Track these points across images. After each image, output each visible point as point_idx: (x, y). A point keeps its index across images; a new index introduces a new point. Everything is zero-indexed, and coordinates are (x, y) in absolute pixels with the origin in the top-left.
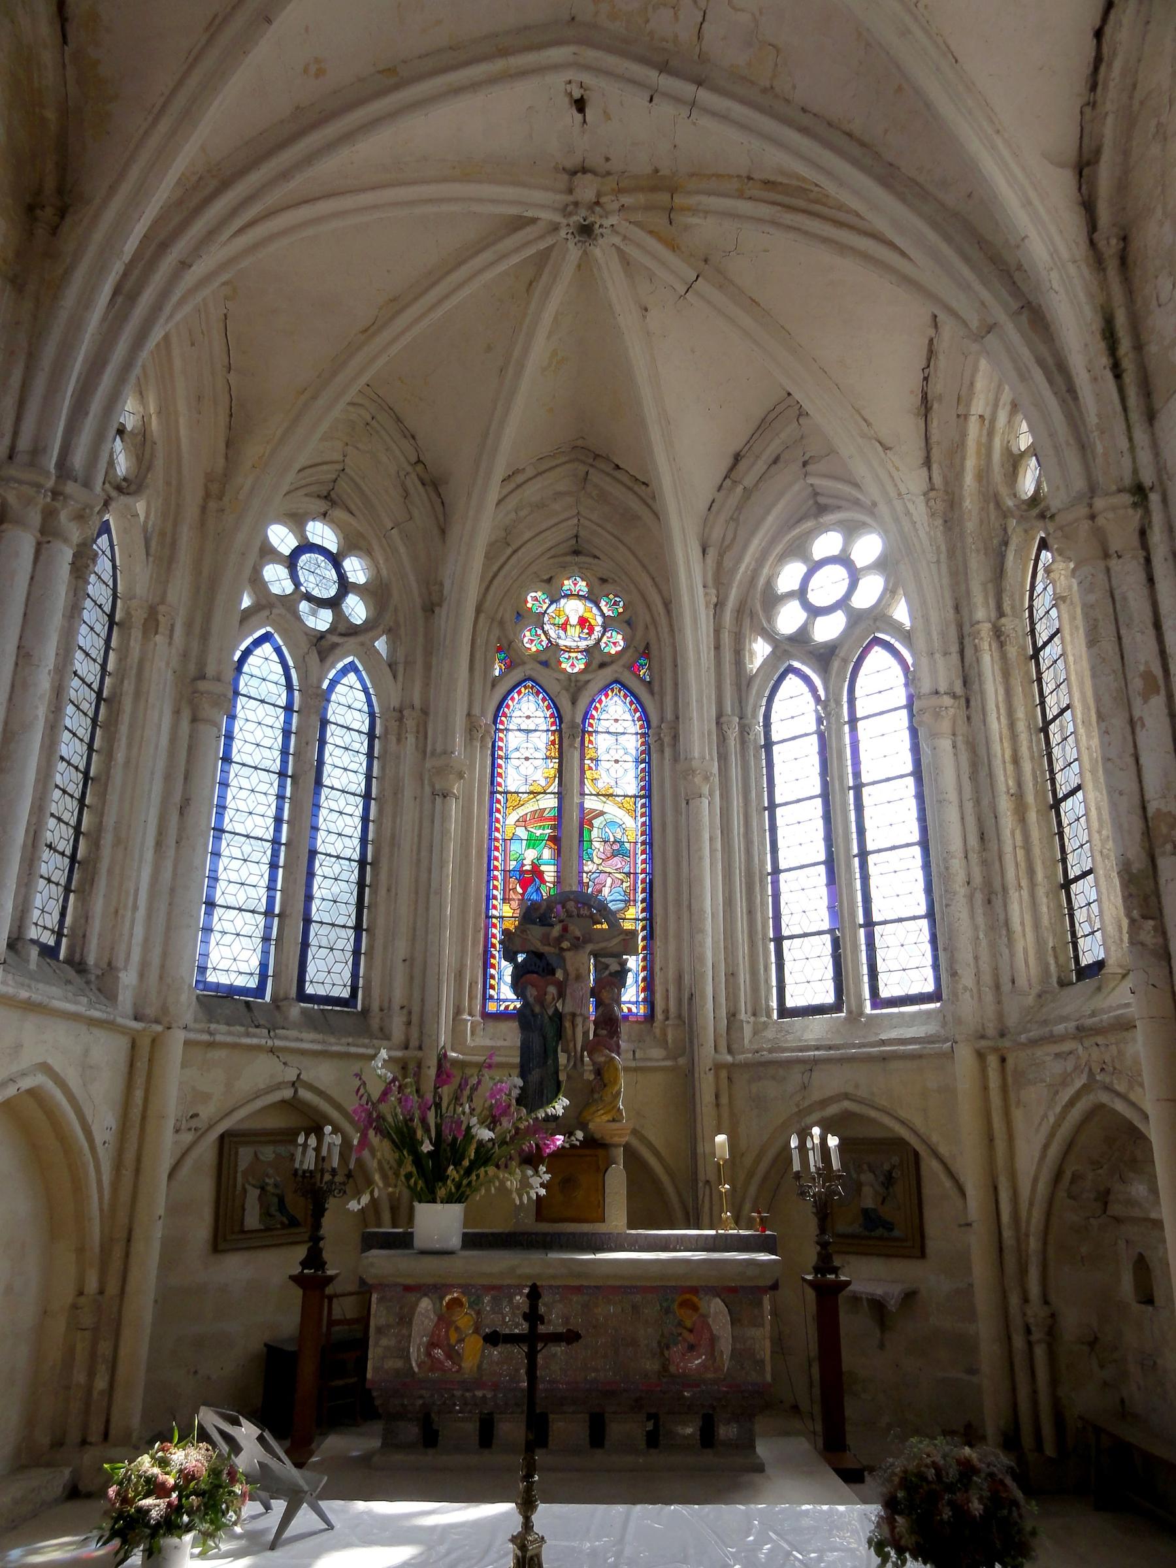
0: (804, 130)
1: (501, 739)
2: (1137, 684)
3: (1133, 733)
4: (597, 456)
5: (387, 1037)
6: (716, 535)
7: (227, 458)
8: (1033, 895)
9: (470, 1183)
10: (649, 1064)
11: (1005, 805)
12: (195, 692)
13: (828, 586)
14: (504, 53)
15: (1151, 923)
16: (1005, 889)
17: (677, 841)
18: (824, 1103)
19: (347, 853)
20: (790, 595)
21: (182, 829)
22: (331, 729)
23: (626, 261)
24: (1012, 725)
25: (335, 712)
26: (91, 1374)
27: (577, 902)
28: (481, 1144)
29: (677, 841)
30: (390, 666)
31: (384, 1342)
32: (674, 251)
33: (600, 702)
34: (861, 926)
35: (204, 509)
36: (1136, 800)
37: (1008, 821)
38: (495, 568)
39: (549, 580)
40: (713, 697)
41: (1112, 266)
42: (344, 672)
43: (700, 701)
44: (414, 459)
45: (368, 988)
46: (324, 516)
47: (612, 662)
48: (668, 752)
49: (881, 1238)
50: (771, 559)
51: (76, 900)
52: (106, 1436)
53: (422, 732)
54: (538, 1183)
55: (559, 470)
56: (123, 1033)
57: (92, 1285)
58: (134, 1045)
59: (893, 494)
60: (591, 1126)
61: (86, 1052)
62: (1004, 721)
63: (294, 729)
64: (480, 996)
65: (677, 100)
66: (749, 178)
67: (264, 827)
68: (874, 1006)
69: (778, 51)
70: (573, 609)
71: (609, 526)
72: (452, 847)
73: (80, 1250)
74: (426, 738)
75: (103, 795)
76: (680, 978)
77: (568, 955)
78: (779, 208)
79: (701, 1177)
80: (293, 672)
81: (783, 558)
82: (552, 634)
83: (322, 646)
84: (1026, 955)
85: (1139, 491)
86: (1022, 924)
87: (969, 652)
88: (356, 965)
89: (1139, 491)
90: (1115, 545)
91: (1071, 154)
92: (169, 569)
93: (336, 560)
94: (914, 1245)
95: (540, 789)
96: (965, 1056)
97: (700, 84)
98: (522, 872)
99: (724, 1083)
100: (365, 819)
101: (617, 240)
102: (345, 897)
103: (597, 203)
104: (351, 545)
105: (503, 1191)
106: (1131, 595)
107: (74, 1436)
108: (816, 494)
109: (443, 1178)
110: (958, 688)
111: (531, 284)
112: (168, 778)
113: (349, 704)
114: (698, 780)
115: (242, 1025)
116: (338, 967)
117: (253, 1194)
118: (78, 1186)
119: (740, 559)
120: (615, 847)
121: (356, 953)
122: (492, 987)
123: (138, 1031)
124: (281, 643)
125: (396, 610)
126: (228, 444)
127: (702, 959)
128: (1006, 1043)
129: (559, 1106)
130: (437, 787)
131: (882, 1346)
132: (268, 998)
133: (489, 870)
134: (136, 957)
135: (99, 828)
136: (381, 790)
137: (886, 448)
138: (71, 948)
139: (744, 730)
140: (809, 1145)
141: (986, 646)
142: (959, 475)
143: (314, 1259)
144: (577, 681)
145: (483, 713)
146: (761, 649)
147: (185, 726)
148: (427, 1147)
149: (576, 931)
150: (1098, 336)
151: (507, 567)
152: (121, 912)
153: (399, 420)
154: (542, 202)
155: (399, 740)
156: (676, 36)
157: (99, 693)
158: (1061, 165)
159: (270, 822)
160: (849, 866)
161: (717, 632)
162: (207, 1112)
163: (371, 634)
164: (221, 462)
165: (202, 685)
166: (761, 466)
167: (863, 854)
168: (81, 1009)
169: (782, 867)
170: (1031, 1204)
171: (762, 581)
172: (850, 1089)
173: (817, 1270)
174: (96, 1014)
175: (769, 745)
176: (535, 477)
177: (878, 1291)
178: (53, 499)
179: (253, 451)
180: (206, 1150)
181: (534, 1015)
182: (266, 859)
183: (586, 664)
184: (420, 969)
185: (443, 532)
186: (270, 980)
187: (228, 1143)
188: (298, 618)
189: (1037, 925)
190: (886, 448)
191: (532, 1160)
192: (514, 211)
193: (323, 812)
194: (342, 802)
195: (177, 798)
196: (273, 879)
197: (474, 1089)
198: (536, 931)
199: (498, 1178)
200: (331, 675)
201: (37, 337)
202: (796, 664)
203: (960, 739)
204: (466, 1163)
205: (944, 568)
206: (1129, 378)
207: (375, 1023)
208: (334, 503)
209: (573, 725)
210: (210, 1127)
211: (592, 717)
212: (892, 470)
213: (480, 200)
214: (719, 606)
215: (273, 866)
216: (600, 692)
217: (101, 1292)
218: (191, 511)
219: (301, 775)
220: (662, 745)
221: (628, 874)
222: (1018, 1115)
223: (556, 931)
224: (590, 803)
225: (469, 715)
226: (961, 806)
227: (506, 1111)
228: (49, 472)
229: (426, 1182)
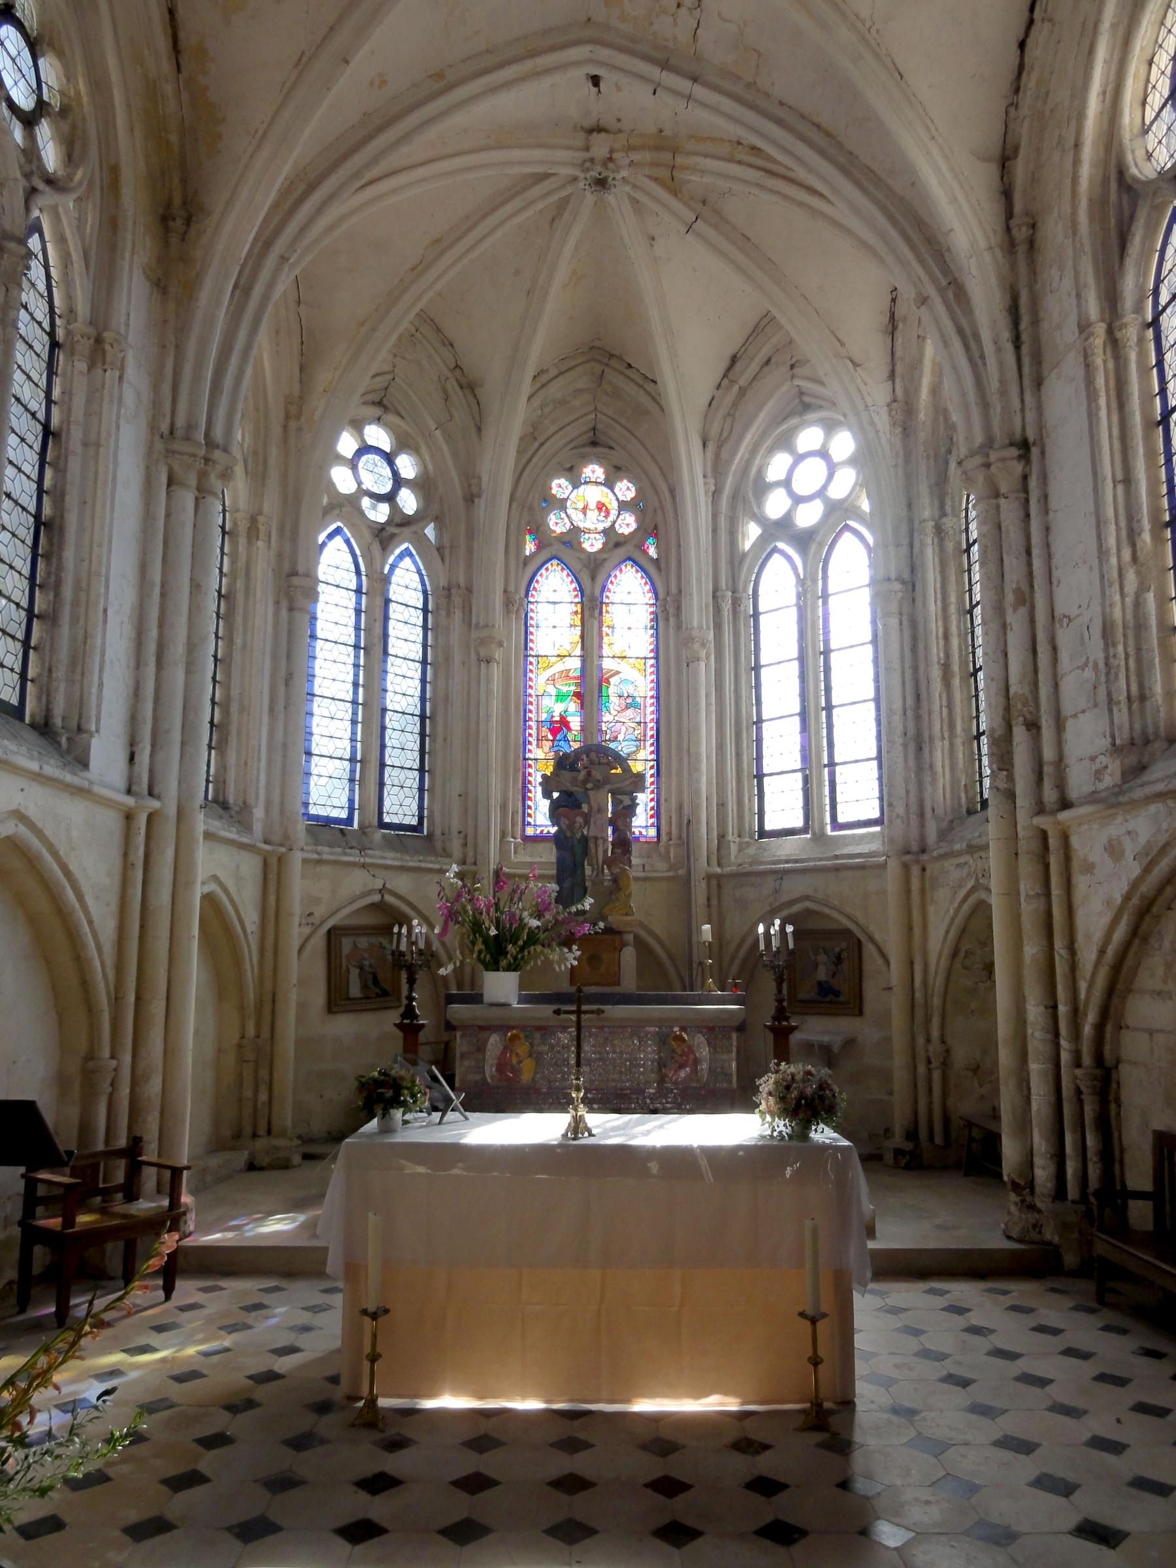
0: (780, 122)
1: (532, 610)
2: (1010, 597)
3: (1005, 634)
4: (611, 356)
6: (714, 431)
7: (301, 382)
8: (952, 745)
9: (523, 957)
10: (655, 875)
11: (936, 673)
12: (290, 586)
13: (809, 477)
14: (533, 54)
15: (1005, 773)
16: (931, 739)
18: (791, 903)
19: (410, 710)
20: (777, 484)
21: (288, 697)
22: (392, 606)
23: (635, 202)
24: (945, 608)
25: (395, 592)
26: (256, 1091)
27: (598, 752)
28: (531, 931)
29: (679, 695)
30: (438, 550)
31: (467, 1063)
32: (676, 195)
33: (615, 576)
34: (825, 766)
35: (285, 427)
36: (1002, 685)
37: (937, 686)
39: (571, 469)
40: (711, 575)
41: (1022, 249)
42: (401, 557)
43: (699, 580)
44: (452, 365)
45: (430, 817)
46: (378, 420)
47: (625, 542)
48: (672, 620)
49: (830, 1002)
50: (762, 451)
51: (216, 755)
52: (269, 1132)
53: (467, 609)
54: (572, 957)
55: (579, 369)
56: (258, 854)
57: (251, 1031)
58: (266, 864)
59: (861, 407)
60: (610, 918)
62: (939, 603)
63: (363, 608)
64: (520, 823)
65: (676, 93)
66: (739, 143)
67: (345, 691)
68: (834, 829)
69: (760, 55)
70: (593, 494)
71: (623, 421)
72: (495, 705)
73: (242, 1008)
74: (471, 612)
75: (228, 675)
76: (680, 807)
77: (591, 793)
78: (762, 173)
79: (695, 959)
80: (360, 560)
81: (771, 451)
82: (574, 517)
83: (383, 537)
84: (941, 791)
85: (1024, 446)
86: (943, 766)
87: (917, 545)
88: (421, 799)
89: (1024, 446)
90: (1004, 489)
91: (996, 150)
92: (263, 485)
93: (389, 459)
94: (857, 1007)
95: (566, 653)
96: (894, 866)
97: (695, 80)
98: (552, 722)
99: (714, 891)
100: (423, 681)
101: (628, 188)
102: (410, 745)
103: (610, 159)
104: (403, 444)
105: (548, 963)
106: (1011, 528)
107: (248, 1130)
108: (801, 393)
109: (504, 953)
110: (906, 576)
111: (553, 220)
112: (275, 656)
113: (406, 583)
114: (696, 646)
115: (339, 847)
116: (408, 801)
118: (238, 963)
119: (733, 454)
120: (629, 701)
121: (421, 789)
122: (530, 815)
123: (268, 852)
124: (349, 535)
125: (441, 500)
126: (302, 369)
127: (697, 793)
128: (925, 857)
130: (482, 654)
132: (356, 826)
133: (525, 721)
134: (262, 798)
135: (228, 698)
136: (435, 656)
137: (856, 365)
138: (216, 791)
139: (736, 602)
140: (772, 932)
141: (929, 541)
142: (917, 390)
143: (409, 1013)
144: (596, 560)
145: (517, 591)
146: (753, 531)
147: (284, 613)
149: (597, 775)
150: (1005, 313)
151: (535, 460)
152: (250, 763)
153: (439, 330)
154: (563, 161)
155: (448, 614)
156: (675, 38)
158: (988, 160)
159: (350, 687)
160: (818, 717)
161: (715, 516)
162: (319, 911)
163: (421, 525)
164: (297, 385)
165: (296, 581)
166: (753, 368)
167: (829, 708)
169: (764, 718)
170: (936, 973)
171: (753, 471)
172: (810, 892)
173: (774, 1018)
175: (756, 615)
176: (557, 376)
177: (826, 1039)
178: (205, 464)
179: (323, 377)
180: (319, 941)
181: (566, 838)
182: (349, 716)
184: (470, 803)
185: (479, 429)
186: (356, 813)
187: (333, 935)
188: (362, 513)
189: (953, 768)
190: (856, 365)
191: (567, 942)
192: (540, 169)
193: (390, 677)
194: (404, 667)
195: (282, 673)
196: (354, 733)
197: (522, 893)
198: (567, 776)
199: (542, 952)
200: (391, 560)
201: (182, 330)
202: (781, 545)
203: (905, 618)
204: (521, 943)
205: (901, 472)
206: (1025, 349)
207: (438, 845)
208: (386, 409)
209: (593, 599)
210: (322, 923)
211: (609, 590)
212: (862, 386)
213: (509, 163)
214: (716, 494)
215: (354, 722)
216: (615, 567)
217: (258, 1036)
218: (276, 431)
219: (372, 645)
220: (668, 614)
221: (639, 723)
222: (931, 909)
223: (582, 775)
225: (505, 591)
226: (903, 673)
227: (547, 908)
228: (200, 444)
229: (492, 956)
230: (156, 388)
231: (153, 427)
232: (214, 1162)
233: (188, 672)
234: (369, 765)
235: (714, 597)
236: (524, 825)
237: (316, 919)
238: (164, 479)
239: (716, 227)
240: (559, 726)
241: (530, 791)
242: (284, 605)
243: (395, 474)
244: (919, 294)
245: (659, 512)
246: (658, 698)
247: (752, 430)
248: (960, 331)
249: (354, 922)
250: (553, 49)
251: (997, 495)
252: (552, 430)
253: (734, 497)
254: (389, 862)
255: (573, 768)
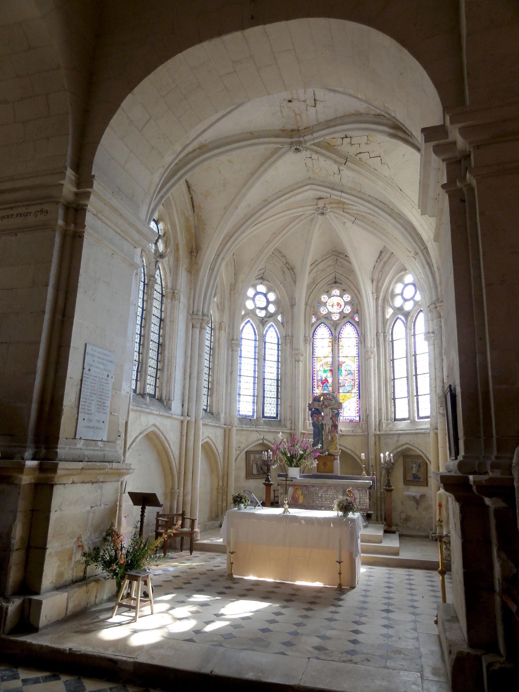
0: (368, 202)
5: (286, 427)
17: (365, 370)
18: (403, 445)
20: (398, 294)
21: (231, 378)
22: (267, 344)
26: (222, 503)
38: (311, 291)
39: (328, 292)
42: (270, 327)
43: (370, 330)
49: (417, 481)
53: (292, 343)
57: (221, 484)
61: (215, 433)
68: (418, 419)
71: (344, 275)
73: (218, 476)
79: (370, 464)
81: (396, 283)
83: (263, 322)
88: (277, 408)
93: (265, 295)
96: (432, 434)
97: (342, 192)
100: (278, 368)
102: (273, 390)
104: (270, 290)
109: (293, 462)
112: (227, 366)
113: (272, 335)
114: (369, 353)
117: (255, 466)
118: (216, 463)
119: (383, 284)
121: (277, 405)
124: (252, 322)
127: (371, 405)
129: (320, 446)
131: (417, 509)
134: (224, 410)
135: (213, 380)
136: (281, 360)
138: (210, 409)
139: (385, 337)
143: (267, 480)
146: (390, 312)
147: (230, 352)
148: (289, 455)
149: (326, 403)
151: (314, 290)
155: (286, 345)
157: (210, 348)
161: (377, 307)
162: (242, 446)
164: (234, 280)
165: (233, 342)
168: (214, 424)
174: (217, 425)
175: (392, 341)
177: (414, 494)
180: (243, 455)
183: (340, 317)
185: (295, 282)
188: (256, 315)
193: (266, 368)
195: (230, 371)
196: (254, 387)
198: (316, 403)
201: (195, 284)
202: (400, 316)
207: (283, 423)
209: (335, 337)
214: (377, 299)
215: (254, 383)
217: (223, 485)
218: (227, 295)
219: (260, 358)
221: (353, 380)
224: (341, 359)
225: (305, 336)
230: (189, 301)
231: (188, 312)
232: (209, 523)
233: (197, 380)
234: (260, 398)
235: (377, 335)
237: (241, 448)
238: (191, 326)
239: (362, 221)
240: (324, 382)
242: (230, 349)
243: (267, 300)
244: (415, 252)
245: (359, 305)
246: (359, 371)
247: (389, 276)
248: (428, 264)
249: (254, 449)
250: (299, 188)
251: (440, 317)
252: (320, 280)
253: (385, 299)
254: (265, 430)
255: (319, 401)
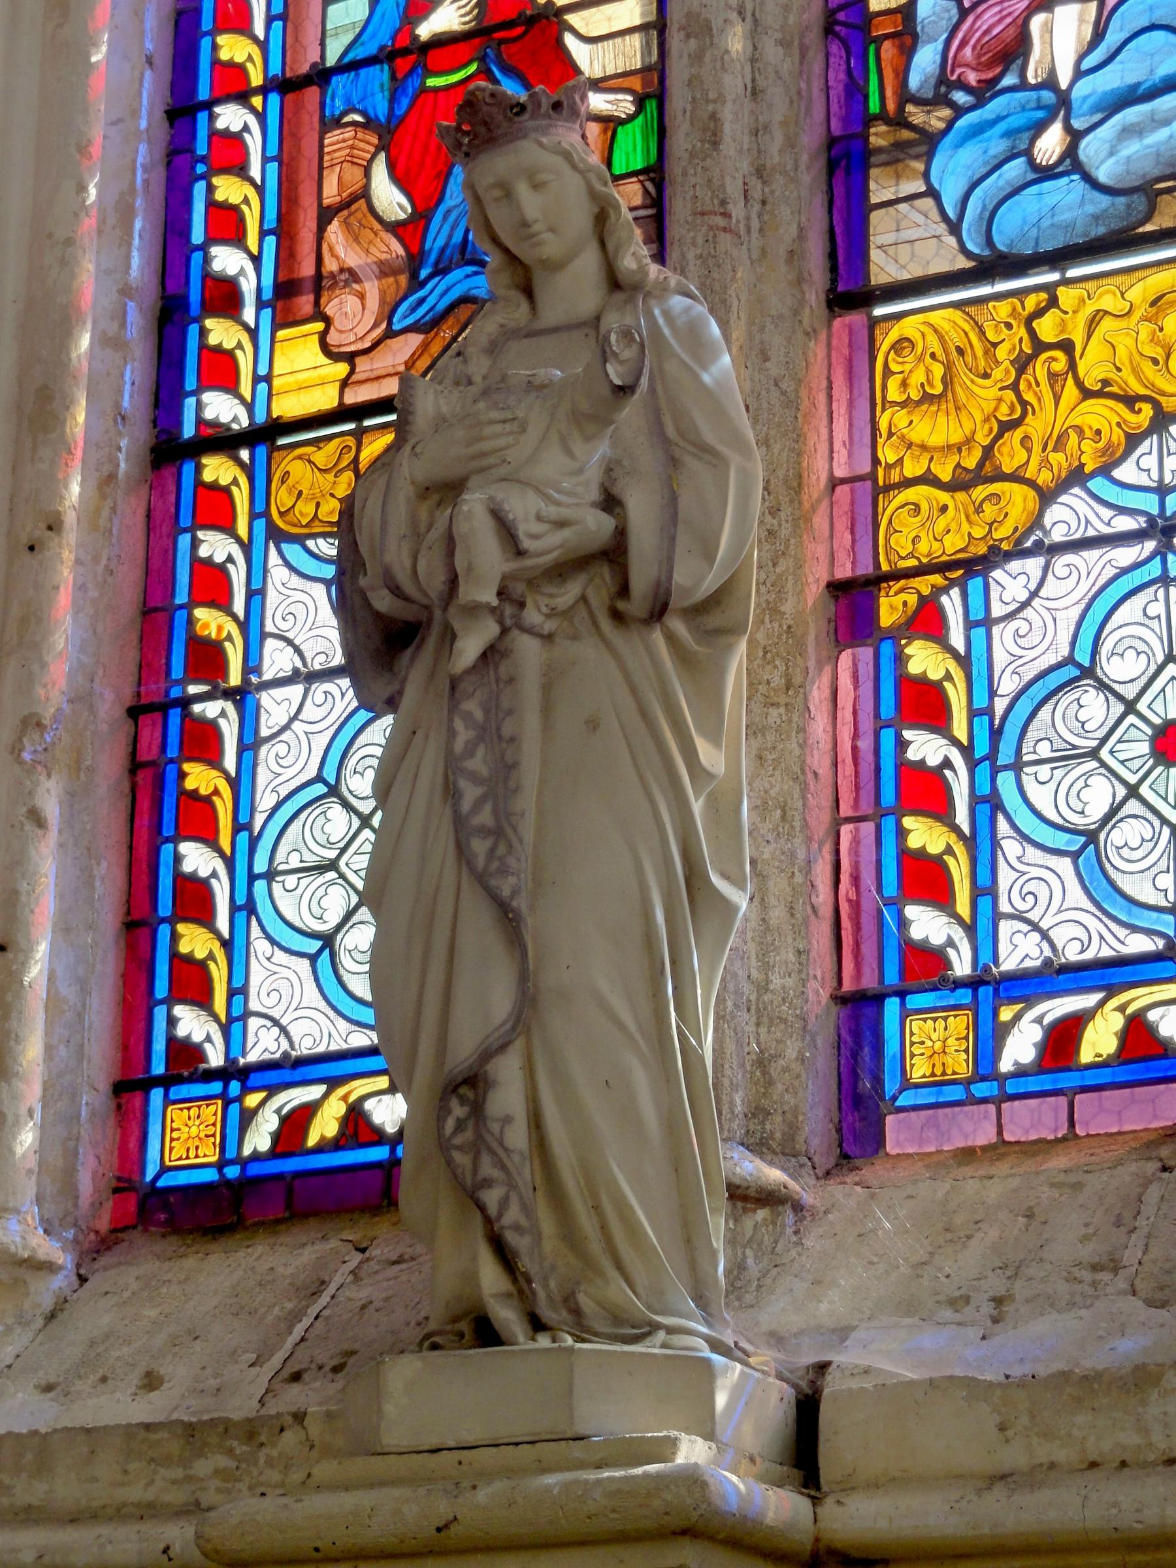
98: (405, 55)
133: (183, 110)
236: (131, 1088)
241: (203, 742)
